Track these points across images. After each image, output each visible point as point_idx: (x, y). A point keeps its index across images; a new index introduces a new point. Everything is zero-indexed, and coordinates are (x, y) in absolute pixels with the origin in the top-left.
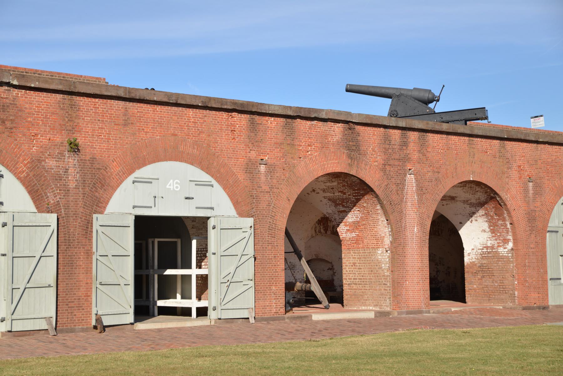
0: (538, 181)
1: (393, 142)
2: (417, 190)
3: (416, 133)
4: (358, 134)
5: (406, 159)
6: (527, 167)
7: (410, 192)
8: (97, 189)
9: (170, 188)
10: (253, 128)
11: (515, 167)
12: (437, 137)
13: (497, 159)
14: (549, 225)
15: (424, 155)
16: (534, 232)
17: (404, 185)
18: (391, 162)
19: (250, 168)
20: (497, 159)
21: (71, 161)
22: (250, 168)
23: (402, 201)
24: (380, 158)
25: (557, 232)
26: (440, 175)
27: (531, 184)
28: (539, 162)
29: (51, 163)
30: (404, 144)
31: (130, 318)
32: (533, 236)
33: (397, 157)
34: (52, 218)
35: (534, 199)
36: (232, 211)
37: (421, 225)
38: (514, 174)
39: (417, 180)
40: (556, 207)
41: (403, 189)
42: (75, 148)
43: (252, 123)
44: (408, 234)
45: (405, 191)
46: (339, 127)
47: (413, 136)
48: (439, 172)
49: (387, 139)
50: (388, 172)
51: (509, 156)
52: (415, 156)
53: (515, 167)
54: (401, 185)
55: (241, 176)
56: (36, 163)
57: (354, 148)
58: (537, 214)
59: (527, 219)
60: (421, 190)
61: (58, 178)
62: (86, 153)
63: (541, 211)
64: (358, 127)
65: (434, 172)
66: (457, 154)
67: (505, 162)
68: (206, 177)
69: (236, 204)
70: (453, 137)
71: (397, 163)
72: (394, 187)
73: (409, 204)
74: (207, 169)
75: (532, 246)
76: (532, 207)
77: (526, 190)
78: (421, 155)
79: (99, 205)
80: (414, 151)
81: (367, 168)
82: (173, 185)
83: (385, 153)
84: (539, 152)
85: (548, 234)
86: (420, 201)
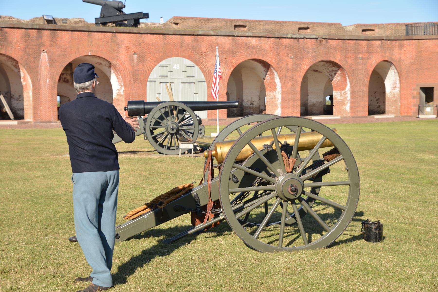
0: (142, 54)
1: (31, 36)
2: (49, 61)
3: (49, 32)
4: (7, 33)
5: (42, 45)
6: (132, 47)
7: (43, 62)
12: (63, 33)
13: (110, 43)
14: (150, 77)
15: (54, 42)
16: (137, 82)
17: (39, 58)
18: (30, 47)
20: (110, 43)
23: (38, 66)
24: (22, 45)
25: (155, 81)
26: (66, 53)
27: (135, 56)
28: (142, 44)
30: (40, 37)
32: (136, 84)
33: (35, 44)
35: (138, 64)
37: (52, 78)
38: (123, 51)
39: (48, 55)
40: (155, 68)
41: (39, 60)
44: (42, 83)
45: (40, 61)
48: (65, 51)
49: (27, 35)
50: (27, 52)
51: (119, 41)
52: (48, 43)
53: (123, 47)
54: (37, 59)
57: (3, 40)
58: (140, 72)
59: (131, 75)
60: (52, 60)
63: (143, 70)
64: (5, 29)
65: (61, 51)
66: (79, 41)
67: (116, 45)
70: (76, 33)
71: (34, 47)
72: (32, 60)
73: (43, 68)
75: (135, 89)
76: (136, 69)
77: (132, 59)
78: (52, 43)
80: (47, 40)
81: (13, 50)
83: (25, 42)
84: (142, 39)
85: (148, 83)
86: (51, 66)
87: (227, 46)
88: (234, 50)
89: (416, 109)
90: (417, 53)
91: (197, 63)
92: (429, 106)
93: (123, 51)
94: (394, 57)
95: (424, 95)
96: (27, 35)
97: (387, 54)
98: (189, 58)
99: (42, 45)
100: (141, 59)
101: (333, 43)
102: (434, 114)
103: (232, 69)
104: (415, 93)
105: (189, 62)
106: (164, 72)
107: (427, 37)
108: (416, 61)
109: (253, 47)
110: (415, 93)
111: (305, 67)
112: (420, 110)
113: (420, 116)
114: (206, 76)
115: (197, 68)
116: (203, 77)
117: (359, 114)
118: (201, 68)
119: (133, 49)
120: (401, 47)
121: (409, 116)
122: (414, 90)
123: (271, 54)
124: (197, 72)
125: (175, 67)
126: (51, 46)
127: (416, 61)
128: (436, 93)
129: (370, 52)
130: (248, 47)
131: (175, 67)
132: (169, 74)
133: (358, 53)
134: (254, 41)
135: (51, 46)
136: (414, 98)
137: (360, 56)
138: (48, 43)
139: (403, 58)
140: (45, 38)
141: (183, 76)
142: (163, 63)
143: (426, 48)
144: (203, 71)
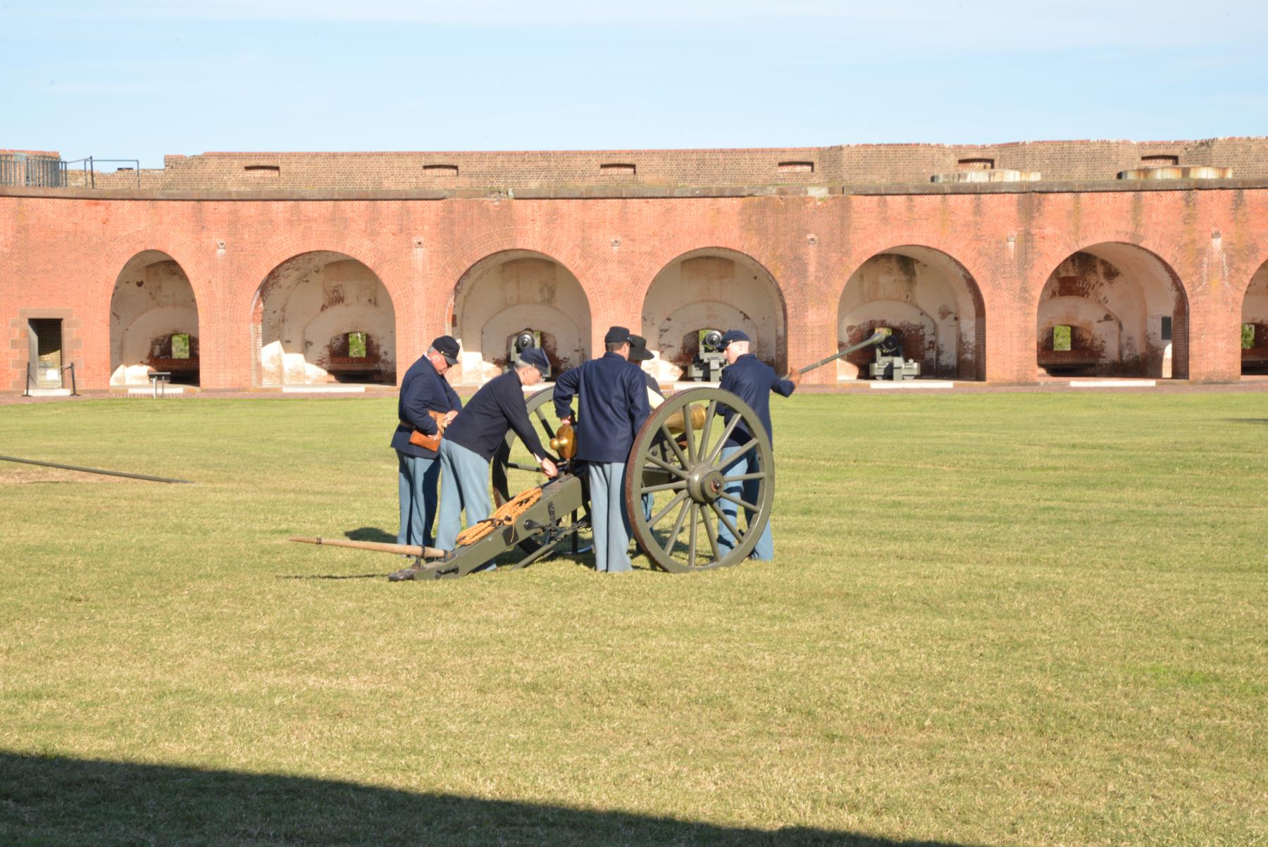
89: (19, 373)
90: (18, 232)
92: (46, 367)
95: (34, 338)
102: (63, 387)
104: (17, 334)
107: (41, 192)
108: (15, 251)
110: (18, 331)
112: (29, 378)
113: (31, 392)
121: (8, 393)
122: (14, 325)
127: (15, 251)
128: (68, 334)
136: (14, 344)
143: (39, 219)
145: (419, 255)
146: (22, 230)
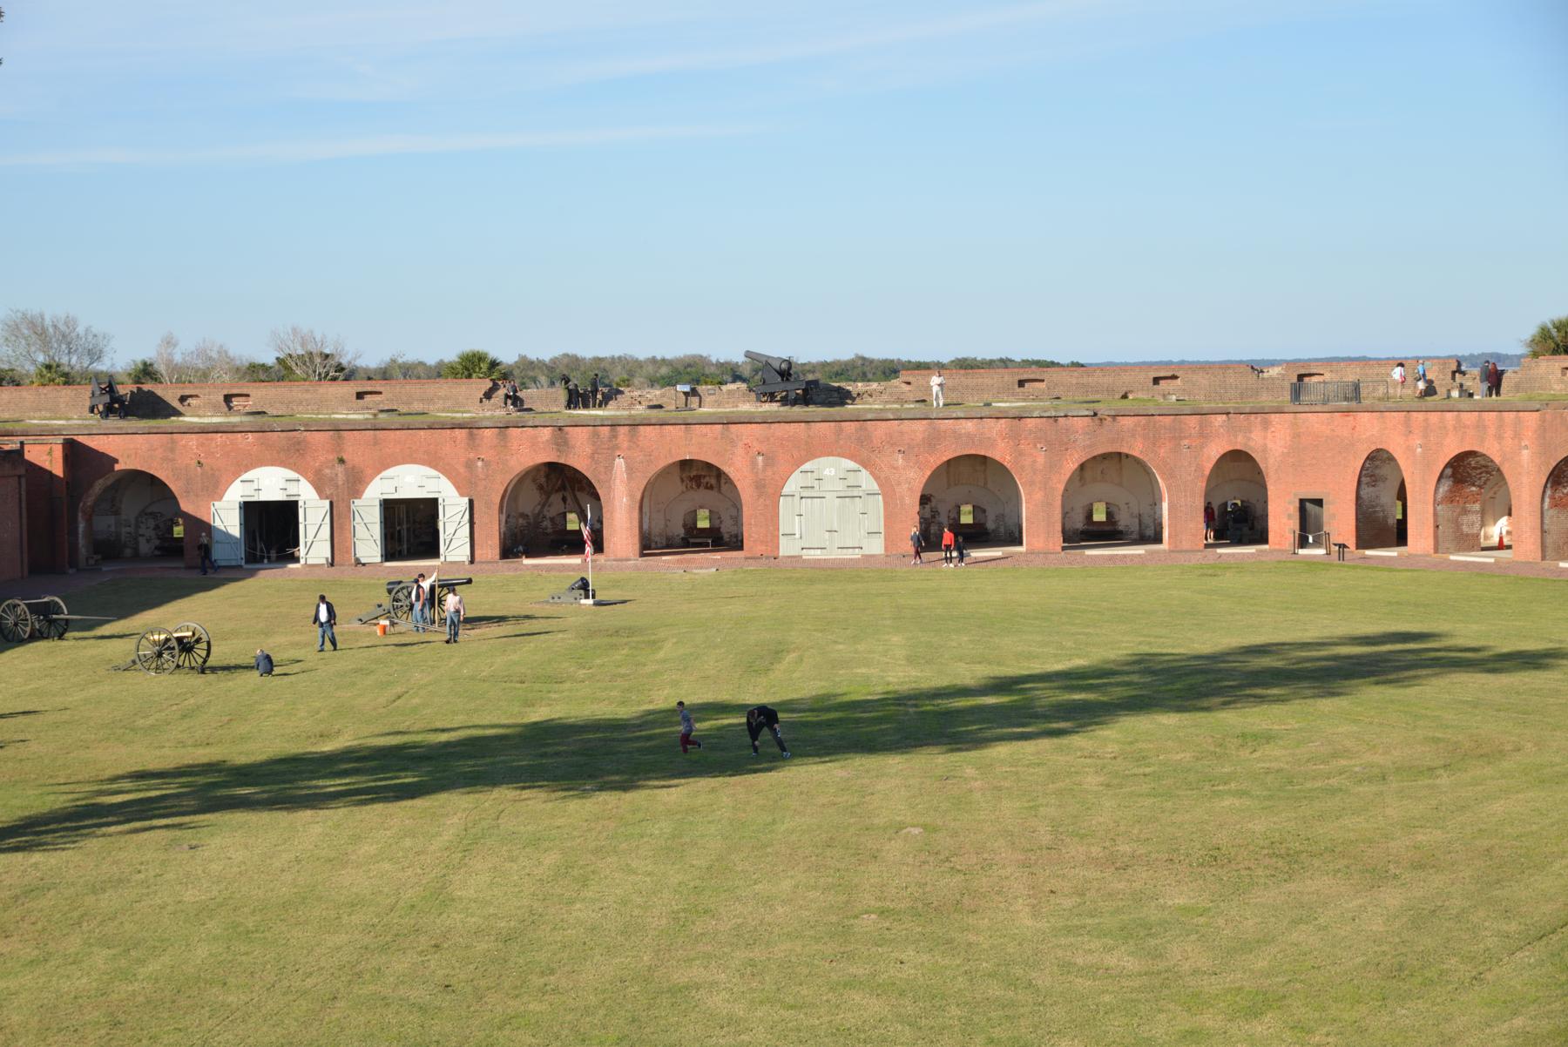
8: (356, 484)
9: (409, 481)
10: (471, 437)
11: (740, 444)
19: (470, 465)
21: (340, 469)
22: (470, 465)
24: (589, 450)
27: (760, 458)
29: (327, 471)
31: (378, 559)
34: (327, 503)
35: (764, 470)
36: (456, 493)
37: (631, 496)
38: (740, 451)
42: (342, 461)
43: (471, 435)
44: (617, 503)
46: (547, 431)
47: (623, 430)
52: (626, 444)
53: (740, 444)
55: (462, 470)
56: (318, 472)
60: (630, 470)
61: (331, 479)
62: (349, 464)
68: (434, 473)
69: (458, 488)
74: (435, 467)
77: (754, 463)
79: (357, 494)
82: (409, 479)
87: (920, 436)
88: (932, 442)
91: (865, 464)
93: (740, 451)
94: (1252, 444)
96: (596, 435)
97: (1240, 438)
98: (852, 457)
99: (616, 447)
100: (770, 461)
101: (1128, 422)
103: (929, 473)
105: (852, 465)
106: (809, 480)
109: (968, 435)
111: (1071, 465)
114: (880, 485)
115: (865, 473)
116: (875, 487)
117: (1186, 545)
118: (872, 474)
119: (757, 446)
120: (1266, 425)
123: (1001, 445)
124: (866, 481)
125: (827, 472)
126: (629, 448)
129: (1204, 435)
130: (957, 436)
131: (827, 472)
132: (816, 483)
133: (1181, 438)
134: (969, 426)
135: (629, 448)
137: (1186, 442)
138: (626, 444)
139: (1270, 445)
140: (621, 437)
141: (841, 486)
142: (807, 466)
144: (877, 478)
145: (1525, 452)
146: (1297, 436)
